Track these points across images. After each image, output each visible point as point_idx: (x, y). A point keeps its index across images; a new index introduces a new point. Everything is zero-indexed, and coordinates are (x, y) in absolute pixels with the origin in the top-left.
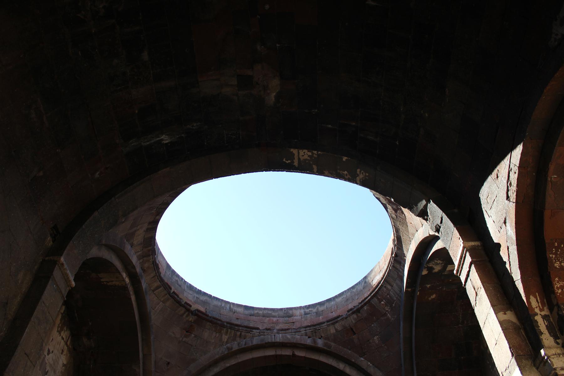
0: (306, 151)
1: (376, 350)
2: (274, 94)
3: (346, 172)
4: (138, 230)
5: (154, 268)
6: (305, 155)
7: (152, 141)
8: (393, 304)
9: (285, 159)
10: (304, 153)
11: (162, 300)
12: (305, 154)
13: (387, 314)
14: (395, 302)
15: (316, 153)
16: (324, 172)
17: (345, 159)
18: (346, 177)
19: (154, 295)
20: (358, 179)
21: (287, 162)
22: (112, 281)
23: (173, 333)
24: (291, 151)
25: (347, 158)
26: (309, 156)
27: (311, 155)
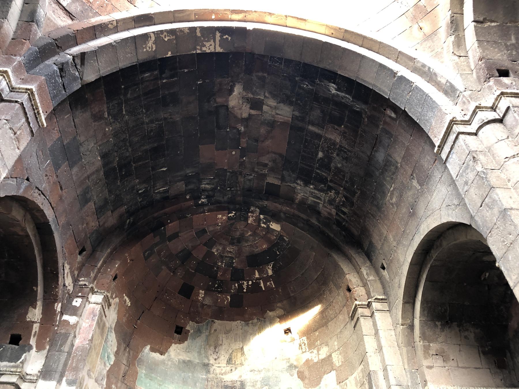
0: (208, 51)
2: (234, 94)
3: (166, 40)
6: (209, 47)
7: (343, 94)
9: (229, 40)
10: (209, 49)
12: (208, 48)
15: (197, 50)
16: (188, 31)
17: (169, 54)
18: (165, 33)
20: (153, 38)
21: (227, 36)
25: (167, 56)
26: (205, 46)
27: (203, 48)
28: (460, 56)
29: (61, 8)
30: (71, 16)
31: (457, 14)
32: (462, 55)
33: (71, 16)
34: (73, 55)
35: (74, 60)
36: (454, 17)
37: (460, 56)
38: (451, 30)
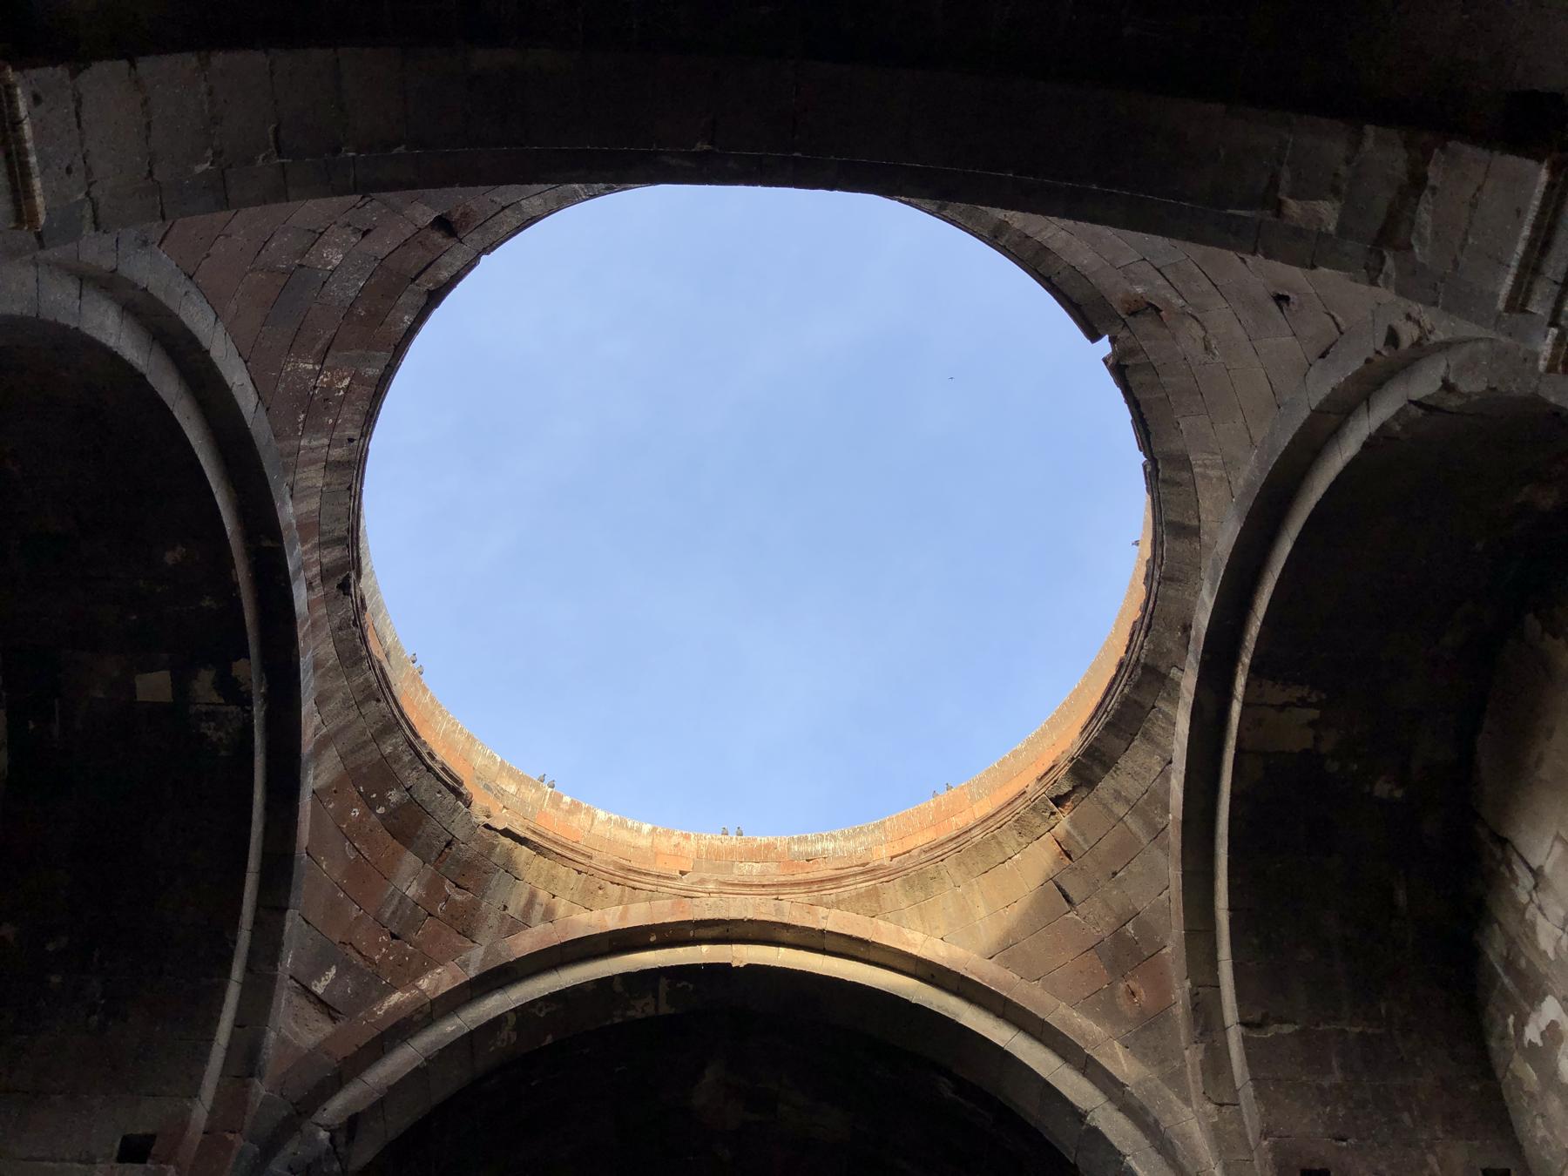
0: (640, 1015)
1: (321, 230)
4: (1127, 801)
5: (1154, 608)
8: (305, 420)
10: (643, 1011)
11: (1185, 475)
12: (640, 1010)
13: (314, 364)
14: (300, 434)
17: (549, 1039)
19: (1203, 517)
21: (685, 983)
22: (1282, 707)
23: (1207, 348)
24: (673, 1009)
28: (1221, 1105)
29: (310, 1002)
30: (331, 1011)
31: (1205, 986)
32: (1226, 1101)
33: (331, 1011)
34: (332, 1127)
35: (332, 1140)
36: (1200, 995)
37: (1221, 1105)
38: (1195, 1030)
